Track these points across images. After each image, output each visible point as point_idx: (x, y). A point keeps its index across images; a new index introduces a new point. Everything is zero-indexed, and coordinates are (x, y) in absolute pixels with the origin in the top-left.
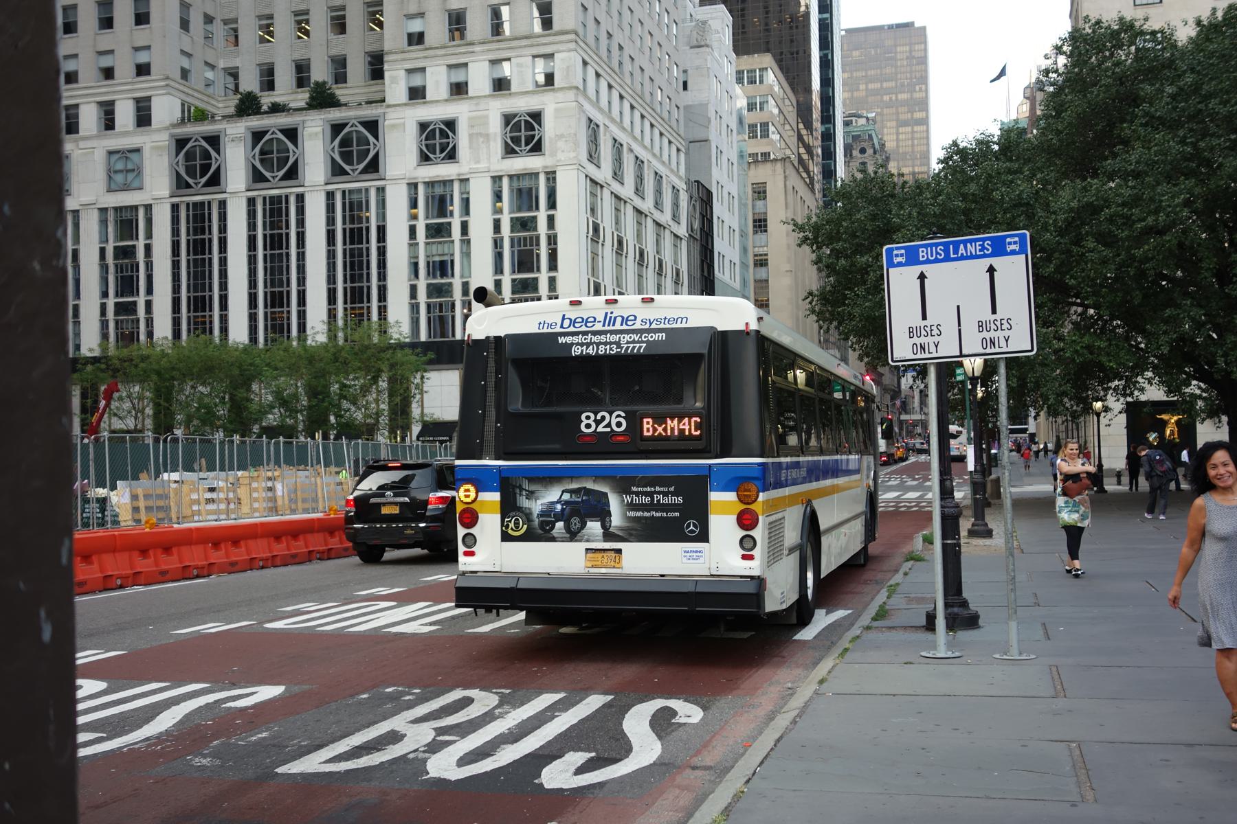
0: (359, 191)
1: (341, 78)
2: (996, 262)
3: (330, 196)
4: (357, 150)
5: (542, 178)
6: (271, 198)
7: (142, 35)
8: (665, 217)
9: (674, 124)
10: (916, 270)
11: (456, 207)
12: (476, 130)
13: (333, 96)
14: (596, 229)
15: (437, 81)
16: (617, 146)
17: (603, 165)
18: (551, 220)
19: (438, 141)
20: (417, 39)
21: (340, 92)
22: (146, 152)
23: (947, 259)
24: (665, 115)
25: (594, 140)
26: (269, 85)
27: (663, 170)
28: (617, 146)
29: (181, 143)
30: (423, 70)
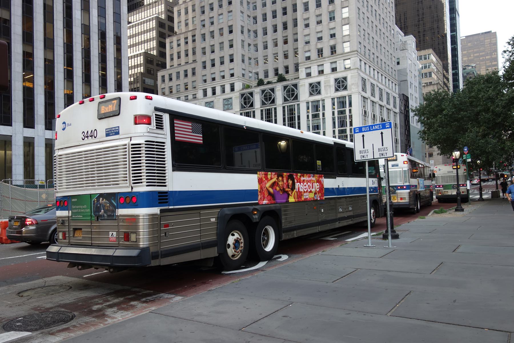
0: (292, 105)
1: (287, 72)
2: (383, 131)
3: (284, 107)
4: (291, 93)
5: (347, 98)
6: (267, 109)
7: (232, 65)
8: (391, 107)
9: (394, 76)
10: (361, 134)
11: (321, 108)
12: (326, 84)
13: (284, 78)
14: (365, 112)
15: (314, 71)
16: (372, 85)
17: (367, 91)
18: (350, 110)
19: (315, 89)
20: (308, 58)
21: (287, 77)
22: (233, 99)
23: (370, 130)
24: (390, 74)
26: (266, 76)
27: (389, 91)
28: (372, 85)
29: (242, 95)
30: (310, 67)
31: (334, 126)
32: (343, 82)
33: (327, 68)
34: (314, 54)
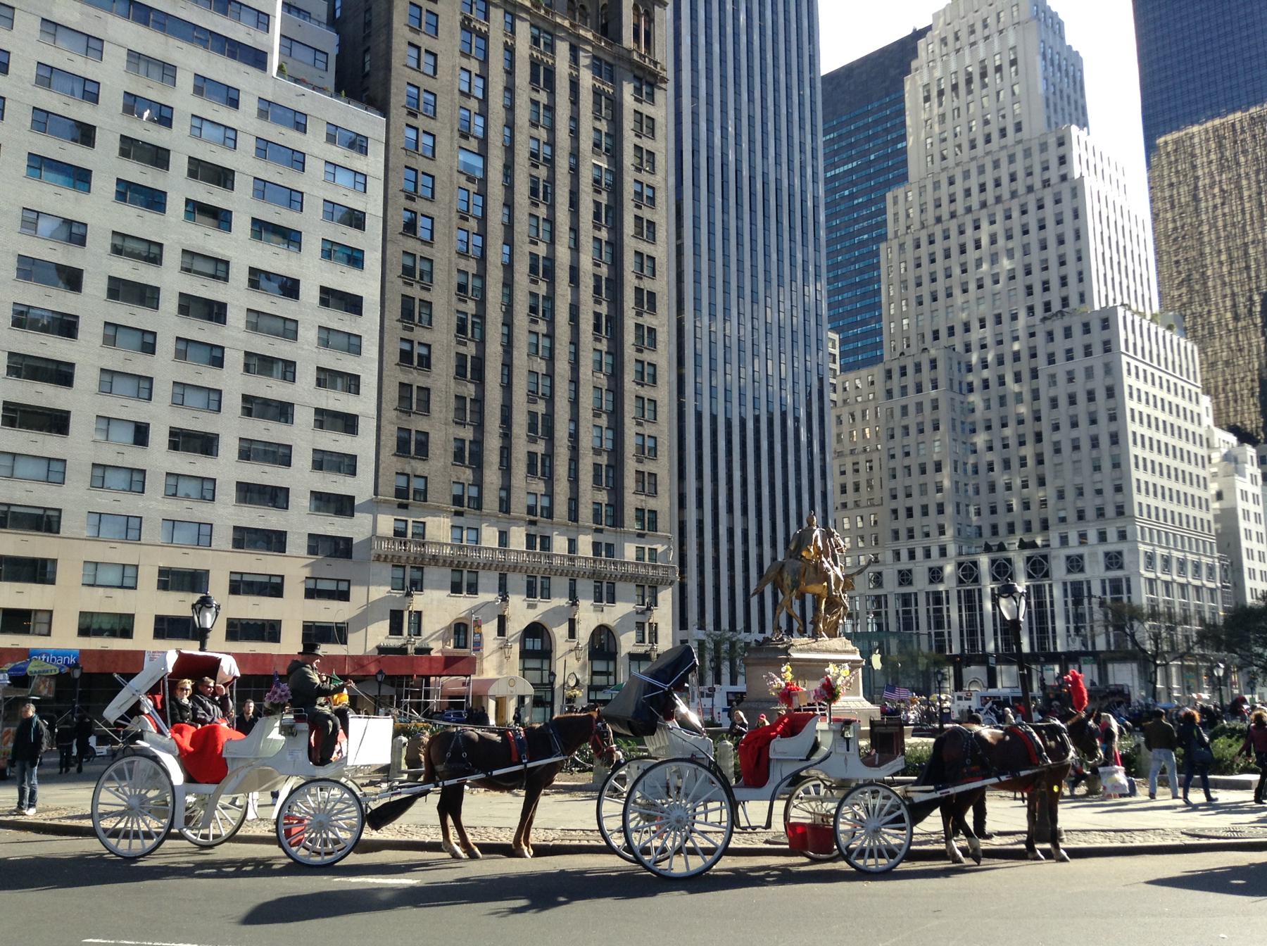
19: (1075, 564)
20: (1063, 520)
33: (1092, 536)
34: (1072, 516)
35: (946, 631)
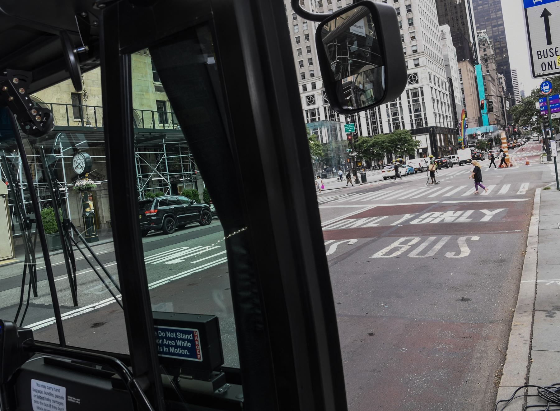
18: (423, 99)
25: (430, 78)
31: (410, 112)
32: (414, 77)
35: (413, 115)
